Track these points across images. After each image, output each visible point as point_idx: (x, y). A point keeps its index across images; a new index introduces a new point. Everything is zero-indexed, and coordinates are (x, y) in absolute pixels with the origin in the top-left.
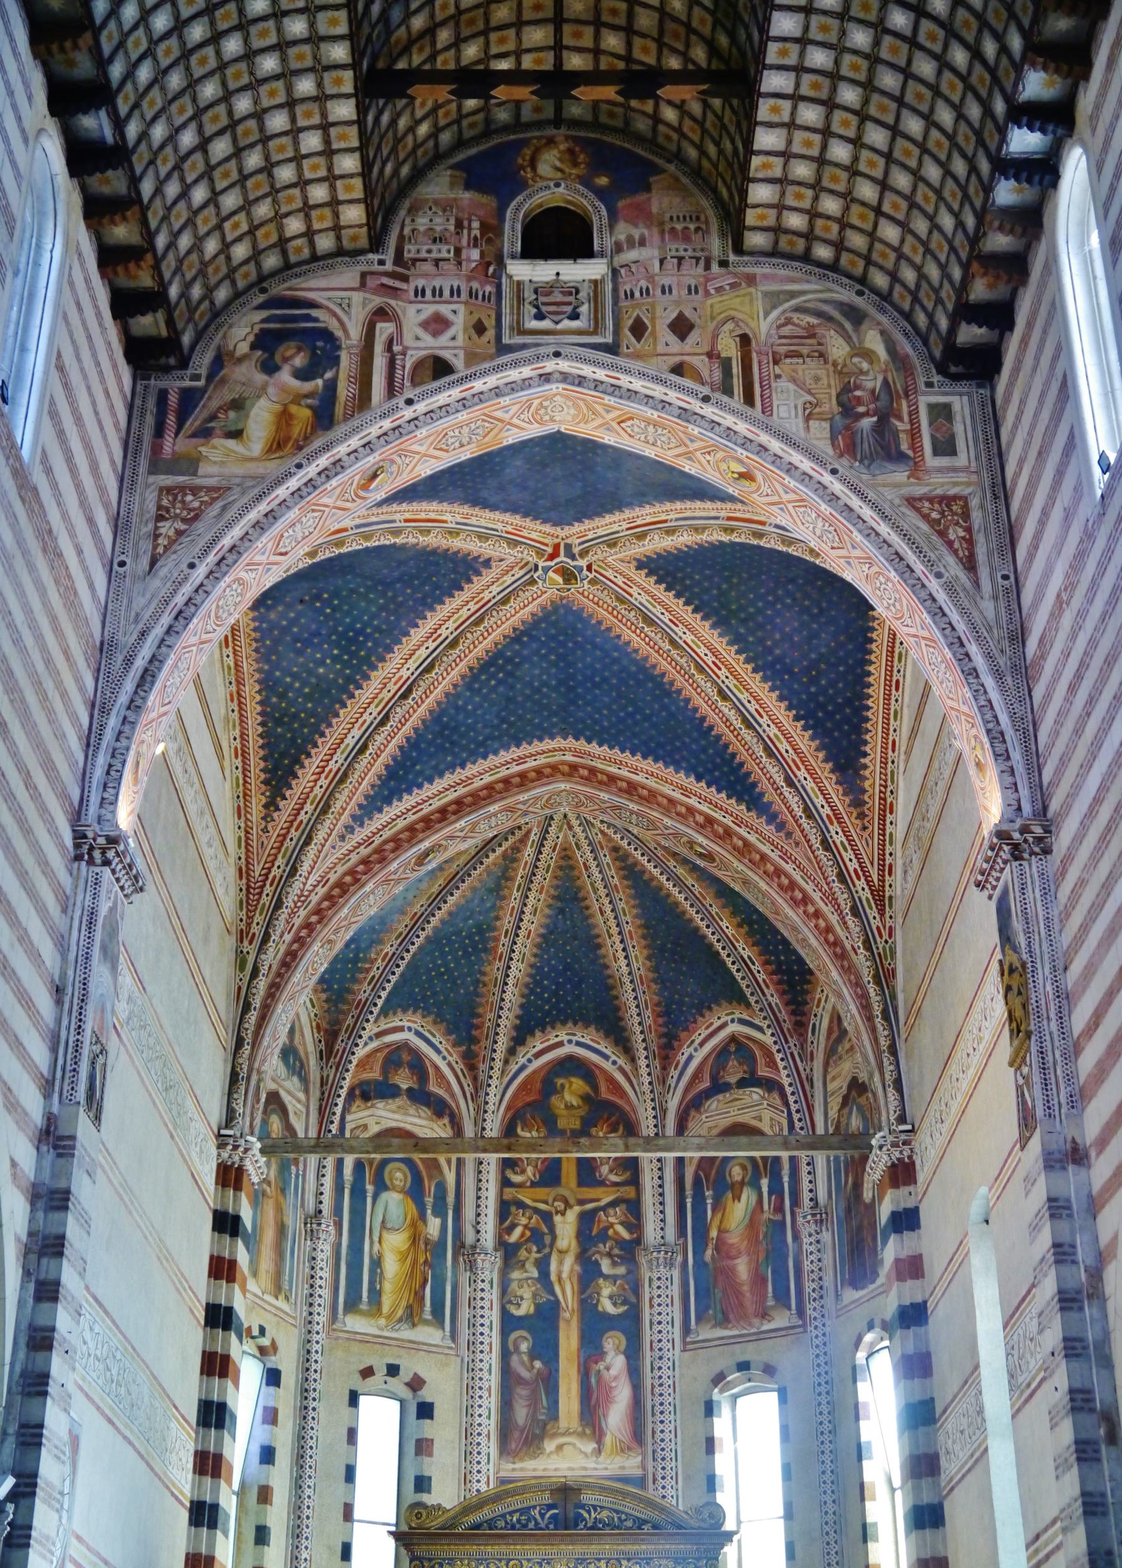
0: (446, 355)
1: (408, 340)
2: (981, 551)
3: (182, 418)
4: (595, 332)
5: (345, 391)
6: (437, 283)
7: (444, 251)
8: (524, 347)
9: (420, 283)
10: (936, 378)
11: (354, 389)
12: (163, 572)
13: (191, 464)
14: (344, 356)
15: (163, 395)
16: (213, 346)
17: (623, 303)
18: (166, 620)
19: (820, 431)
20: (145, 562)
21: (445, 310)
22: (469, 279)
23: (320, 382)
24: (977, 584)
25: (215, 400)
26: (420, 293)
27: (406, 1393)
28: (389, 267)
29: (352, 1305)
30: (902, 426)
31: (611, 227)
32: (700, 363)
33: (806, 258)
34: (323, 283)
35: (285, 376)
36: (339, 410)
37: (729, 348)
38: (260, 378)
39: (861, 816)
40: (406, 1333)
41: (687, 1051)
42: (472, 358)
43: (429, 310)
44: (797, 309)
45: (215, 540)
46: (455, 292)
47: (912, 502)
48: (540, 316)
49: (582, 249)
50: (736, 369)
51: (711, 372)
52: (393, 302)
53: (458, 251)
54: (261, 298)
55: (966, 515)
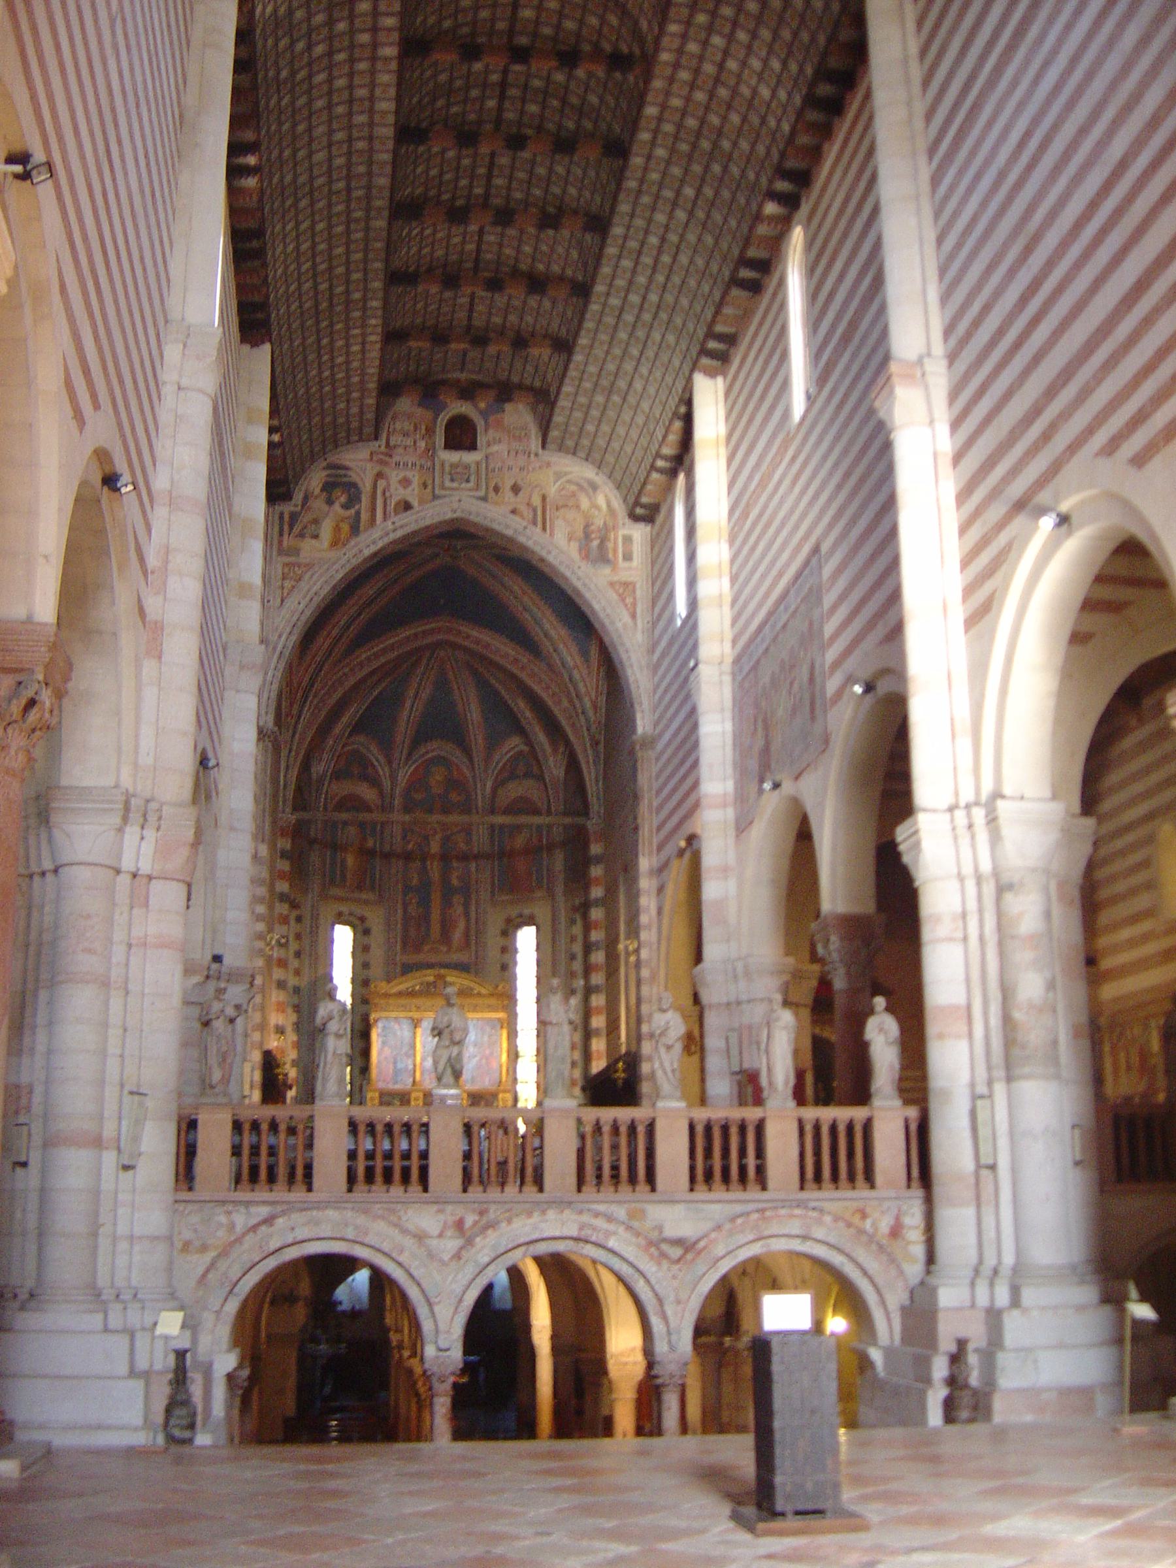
2: (639, 611)
4: (477, 490)
5: (364, 516)
6: (405, 459)
8: (445, 496)
10: (627, 520)
11: (369, 514)
12: (288, 603)
13: (296, 551)
14: (364, 499)
16: (303, 489)
17: (490, 475)
21: (409, 474)
22: (421, 457)
23: (353, 511)
24: (636, 624)
25: (306, 518)
26: (397, 464)
27: (357, 922)
29: (332, 882)
30: (610, 545)
31: (486, 430)
32: (523, 508)
34: (352, 457)
35: (337, 507)
36: (362, 528)
37: (536, 501)
38: (325, 508)
39: (588, 667)
40: (356, 895)
41: (496, 757)
43: (402, 475)
44: (569, 481)
47: (612, 584)
48: (452, 480)
50: (539, 513)
51: (528, 514)
52: (386, 470)
53: (415, 442)
54: (325, 464)
55: (634, 591)
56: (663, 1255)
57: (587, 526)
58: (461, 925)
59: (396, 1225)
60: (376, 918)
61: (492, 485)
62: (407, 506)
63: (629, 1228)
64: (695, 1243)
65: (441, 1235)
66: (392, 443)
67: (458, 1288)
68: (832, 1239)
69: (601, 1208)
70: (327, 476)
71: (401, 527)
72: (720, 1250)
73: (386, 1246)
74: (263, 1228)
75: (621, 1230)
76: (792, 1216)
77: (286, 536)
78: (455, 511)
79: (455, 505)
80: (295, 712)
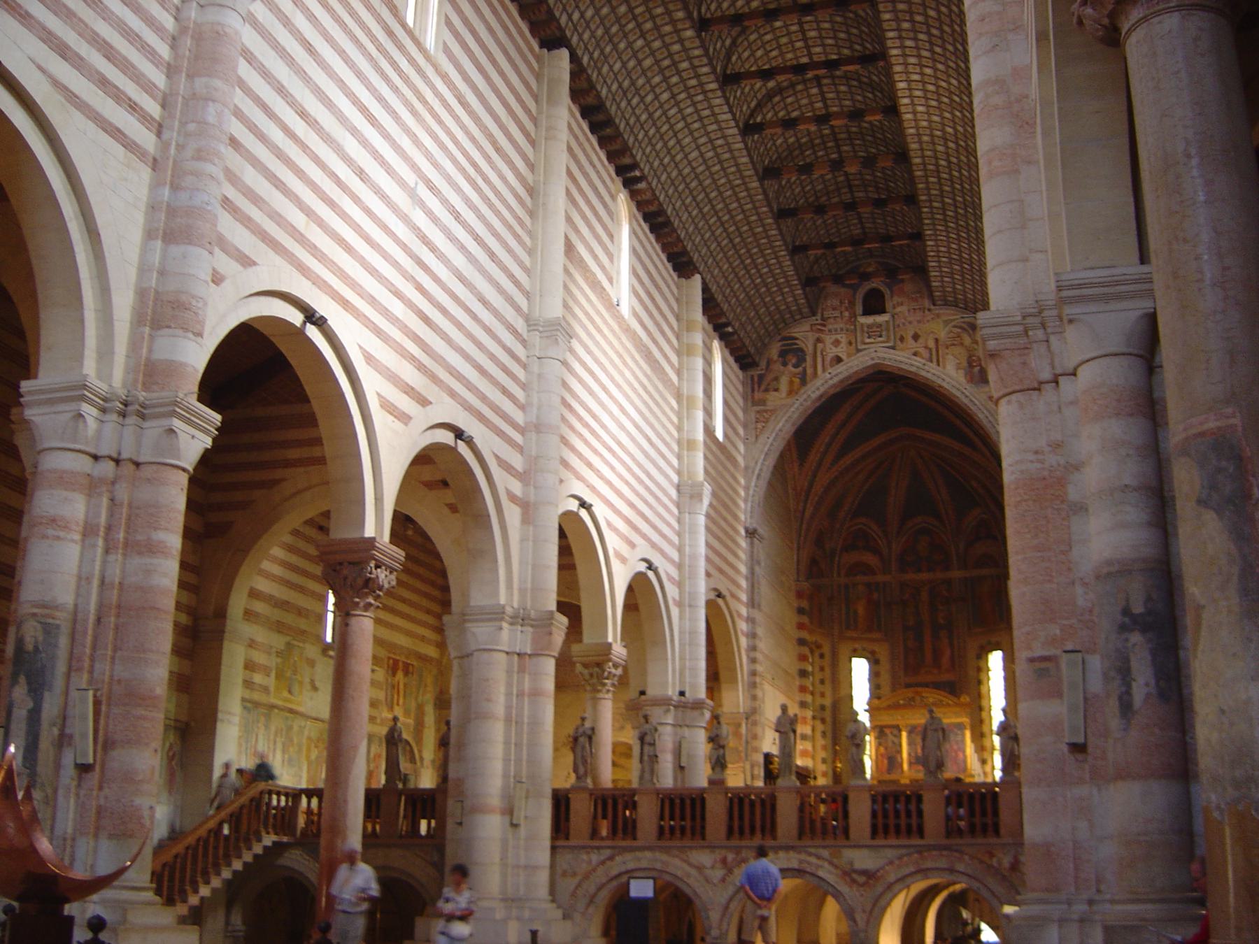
0: (840, 355)
1: (829, 351)
3: (759, 387)
5: (809, 371)
6: (835, 326)
7: (837, 314)
9: (830, 327)
13: (763, 402)
15: (752, 377)
18: (762, 457)
19: (961, 372)
20: (754, 439)
21: (838, 337)
23: (801, 369)
25: (770, 377)
26: (830, 331)
27: (869, 656)
28: (819, 322)
31: (892, 297)
32: (922, 350)
33: (957, 306)
35: (790, 367)
36: (808, 379)
37: (931, 344)
42: (849, 355)
44: (955, 327)
45: (774, 429)
46: (842, 329)
48: (869, 337)
49: (883, 311)
54: (779, 337)
56: (854, 881)
57: (970, 357)
58: (947, 653)
59: (685, 861)
60: (883, 651)
61: (898, 337)
62: (839, 360)
63: (831, 863)
64: (875, 873)
65: (713, 867)
66: (826, 316)
67: (723, 901)
68: (970, 872)
69: (813, 850)
70: (783, 345)
71: (836, 375)
72: (892, 878)
73: (679, 873)
74: (608, 863)
75: (826, 864)
76: (942, 855)
77: (756, 393)
78: (873, 359)
79: (874, 355)
80: (801, 508)
